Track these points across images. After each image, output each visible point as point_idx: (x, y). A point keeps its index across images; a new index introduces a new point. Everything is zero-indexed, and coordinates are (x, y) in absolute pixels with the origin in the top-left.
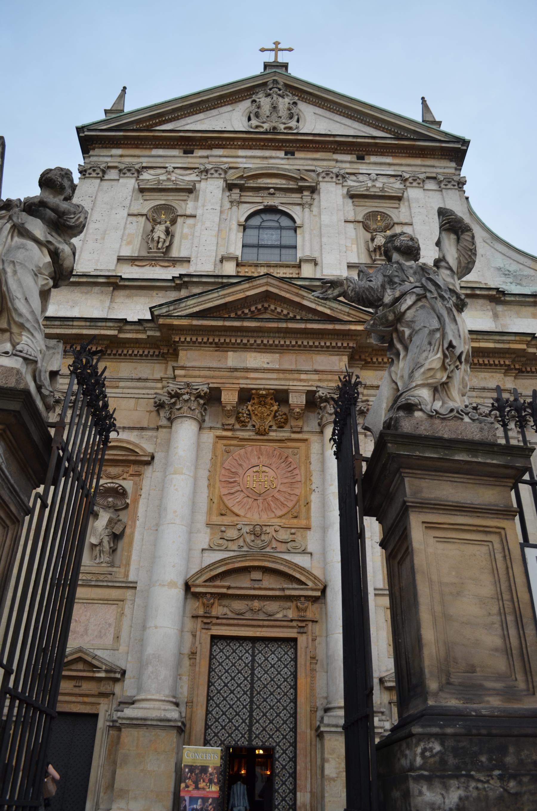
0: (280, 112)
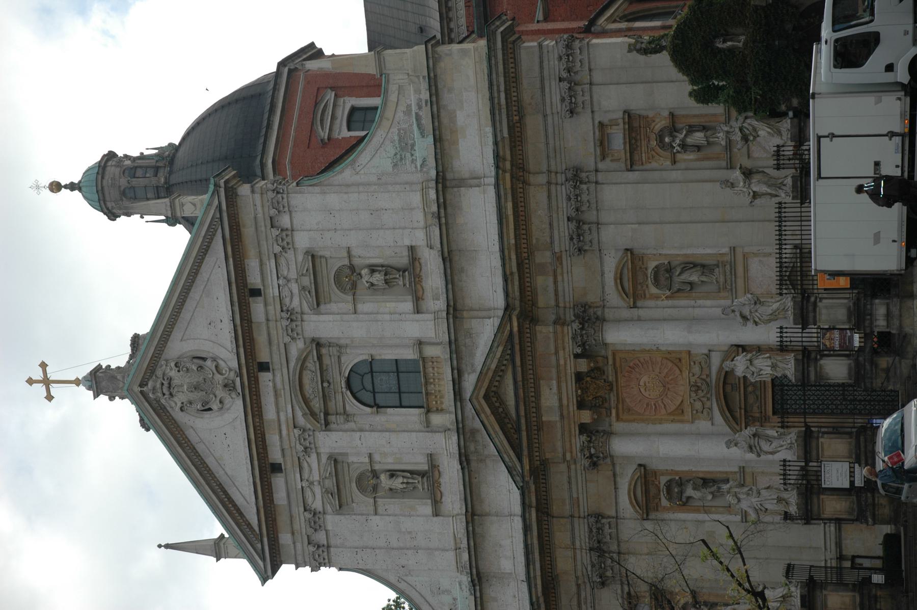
0: (196, 380)
